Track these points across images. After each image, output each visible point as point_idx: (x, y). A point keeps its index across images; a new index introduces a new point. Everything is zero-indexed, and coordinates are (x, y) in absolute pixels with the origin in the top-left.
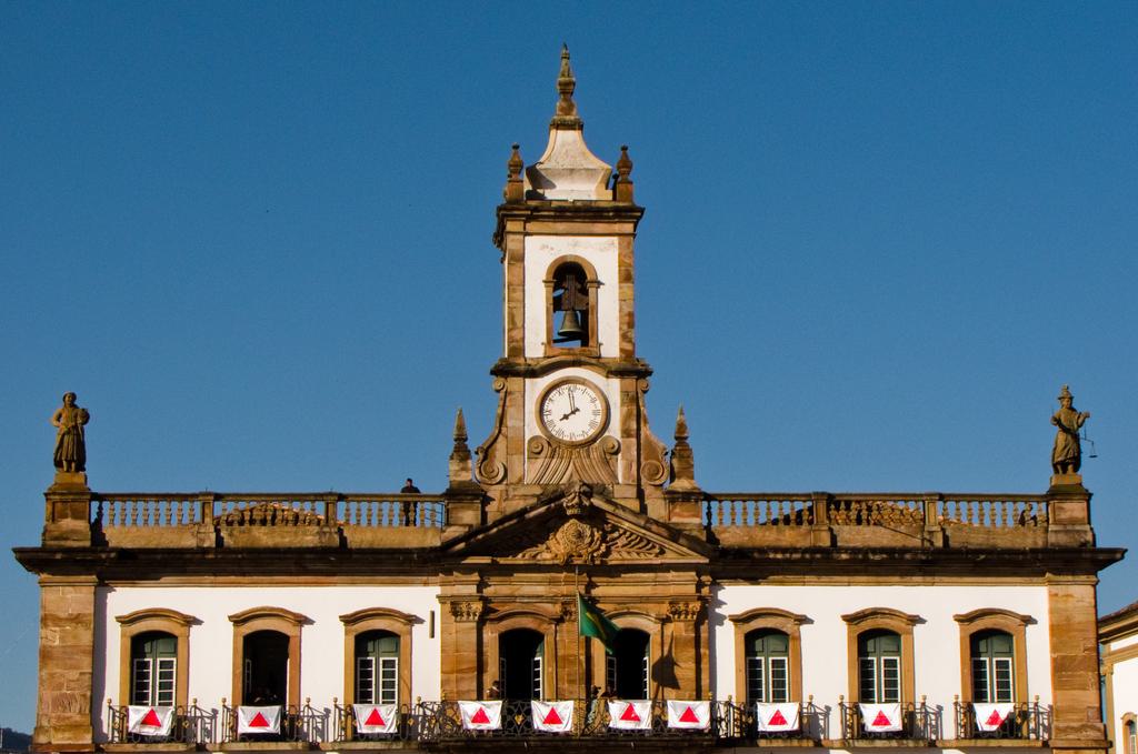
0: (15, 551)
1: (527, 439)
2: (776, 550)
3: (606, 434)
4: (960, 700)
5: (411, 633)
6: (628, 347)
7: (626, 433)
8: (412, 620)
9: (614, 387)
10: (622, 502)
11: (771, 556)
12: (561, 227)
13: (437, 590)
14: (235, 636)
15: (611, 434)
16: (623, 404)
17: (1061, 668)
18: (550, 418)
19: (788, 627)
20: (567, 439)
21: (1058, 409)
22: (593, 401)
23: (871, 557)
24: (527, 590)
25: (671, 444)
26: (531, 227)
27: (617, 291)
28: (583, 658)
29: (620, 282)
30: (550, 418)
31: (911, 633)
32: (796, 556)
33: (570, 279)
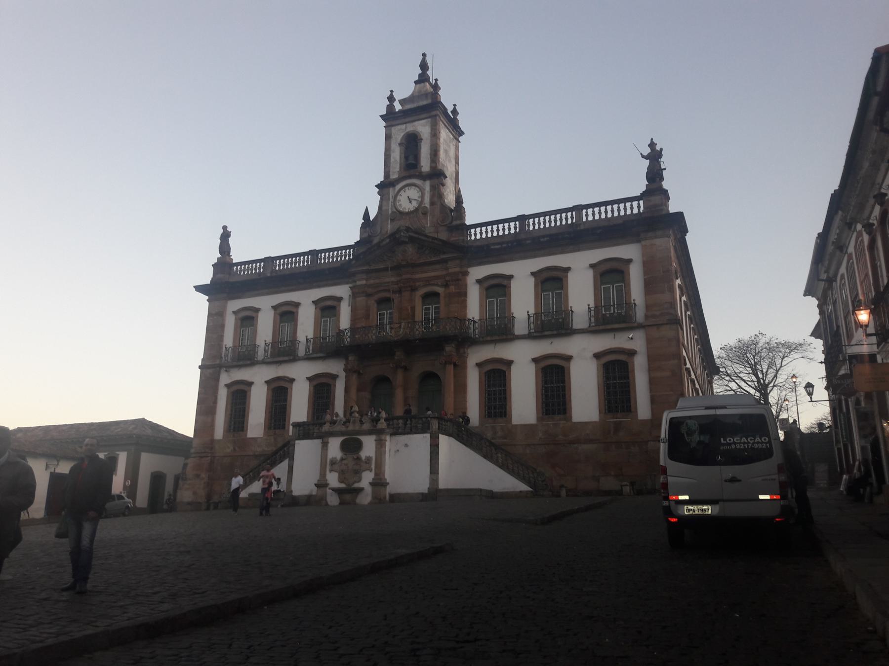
0: (194, 287)
1: (390, 212)
2: (494, 244)
3: (423, 205)
4: (592, 305)
5: (340, 305)
6: (434, 165)
7: (432, 203)
8: (340, 299)
9: (427, 185)
10: (428, 235)
11: (492, 247)
12: (407, 120)
13: (351, 285)
14: (275, 314)
15: (426, 205)
16: (430, 192)
17: (650, 286)
18: (400, 203)
19: (505, 282)
20: (407, 211)
21: (649, 150)
22: (418, 192)
23: (542, 240)
24: (387, 280)
25: (452, 205)
26: (394, 123)
27: (429, 141)
28: (409, 308)
29: (431, 137)
30: (400, 203)
31: (567, 277)
32: (504, 245)
33: (412, 142)
